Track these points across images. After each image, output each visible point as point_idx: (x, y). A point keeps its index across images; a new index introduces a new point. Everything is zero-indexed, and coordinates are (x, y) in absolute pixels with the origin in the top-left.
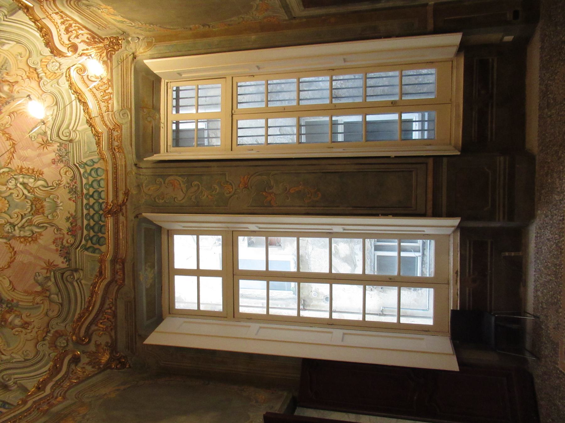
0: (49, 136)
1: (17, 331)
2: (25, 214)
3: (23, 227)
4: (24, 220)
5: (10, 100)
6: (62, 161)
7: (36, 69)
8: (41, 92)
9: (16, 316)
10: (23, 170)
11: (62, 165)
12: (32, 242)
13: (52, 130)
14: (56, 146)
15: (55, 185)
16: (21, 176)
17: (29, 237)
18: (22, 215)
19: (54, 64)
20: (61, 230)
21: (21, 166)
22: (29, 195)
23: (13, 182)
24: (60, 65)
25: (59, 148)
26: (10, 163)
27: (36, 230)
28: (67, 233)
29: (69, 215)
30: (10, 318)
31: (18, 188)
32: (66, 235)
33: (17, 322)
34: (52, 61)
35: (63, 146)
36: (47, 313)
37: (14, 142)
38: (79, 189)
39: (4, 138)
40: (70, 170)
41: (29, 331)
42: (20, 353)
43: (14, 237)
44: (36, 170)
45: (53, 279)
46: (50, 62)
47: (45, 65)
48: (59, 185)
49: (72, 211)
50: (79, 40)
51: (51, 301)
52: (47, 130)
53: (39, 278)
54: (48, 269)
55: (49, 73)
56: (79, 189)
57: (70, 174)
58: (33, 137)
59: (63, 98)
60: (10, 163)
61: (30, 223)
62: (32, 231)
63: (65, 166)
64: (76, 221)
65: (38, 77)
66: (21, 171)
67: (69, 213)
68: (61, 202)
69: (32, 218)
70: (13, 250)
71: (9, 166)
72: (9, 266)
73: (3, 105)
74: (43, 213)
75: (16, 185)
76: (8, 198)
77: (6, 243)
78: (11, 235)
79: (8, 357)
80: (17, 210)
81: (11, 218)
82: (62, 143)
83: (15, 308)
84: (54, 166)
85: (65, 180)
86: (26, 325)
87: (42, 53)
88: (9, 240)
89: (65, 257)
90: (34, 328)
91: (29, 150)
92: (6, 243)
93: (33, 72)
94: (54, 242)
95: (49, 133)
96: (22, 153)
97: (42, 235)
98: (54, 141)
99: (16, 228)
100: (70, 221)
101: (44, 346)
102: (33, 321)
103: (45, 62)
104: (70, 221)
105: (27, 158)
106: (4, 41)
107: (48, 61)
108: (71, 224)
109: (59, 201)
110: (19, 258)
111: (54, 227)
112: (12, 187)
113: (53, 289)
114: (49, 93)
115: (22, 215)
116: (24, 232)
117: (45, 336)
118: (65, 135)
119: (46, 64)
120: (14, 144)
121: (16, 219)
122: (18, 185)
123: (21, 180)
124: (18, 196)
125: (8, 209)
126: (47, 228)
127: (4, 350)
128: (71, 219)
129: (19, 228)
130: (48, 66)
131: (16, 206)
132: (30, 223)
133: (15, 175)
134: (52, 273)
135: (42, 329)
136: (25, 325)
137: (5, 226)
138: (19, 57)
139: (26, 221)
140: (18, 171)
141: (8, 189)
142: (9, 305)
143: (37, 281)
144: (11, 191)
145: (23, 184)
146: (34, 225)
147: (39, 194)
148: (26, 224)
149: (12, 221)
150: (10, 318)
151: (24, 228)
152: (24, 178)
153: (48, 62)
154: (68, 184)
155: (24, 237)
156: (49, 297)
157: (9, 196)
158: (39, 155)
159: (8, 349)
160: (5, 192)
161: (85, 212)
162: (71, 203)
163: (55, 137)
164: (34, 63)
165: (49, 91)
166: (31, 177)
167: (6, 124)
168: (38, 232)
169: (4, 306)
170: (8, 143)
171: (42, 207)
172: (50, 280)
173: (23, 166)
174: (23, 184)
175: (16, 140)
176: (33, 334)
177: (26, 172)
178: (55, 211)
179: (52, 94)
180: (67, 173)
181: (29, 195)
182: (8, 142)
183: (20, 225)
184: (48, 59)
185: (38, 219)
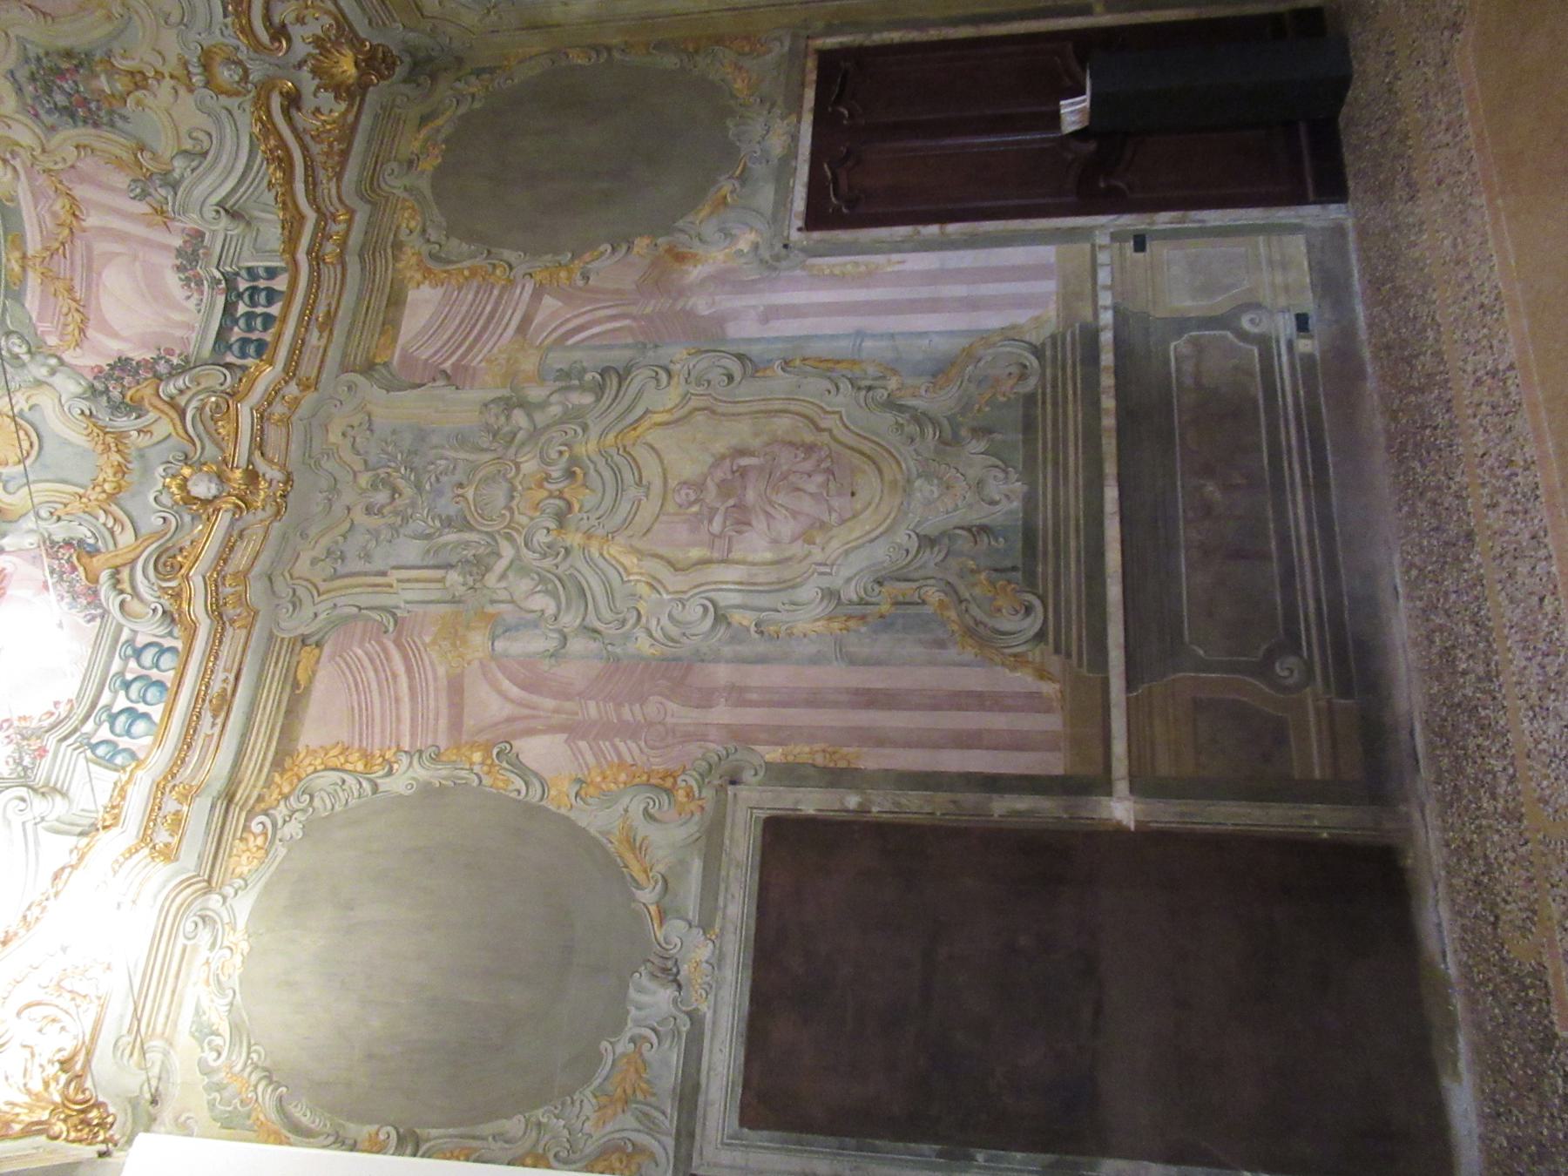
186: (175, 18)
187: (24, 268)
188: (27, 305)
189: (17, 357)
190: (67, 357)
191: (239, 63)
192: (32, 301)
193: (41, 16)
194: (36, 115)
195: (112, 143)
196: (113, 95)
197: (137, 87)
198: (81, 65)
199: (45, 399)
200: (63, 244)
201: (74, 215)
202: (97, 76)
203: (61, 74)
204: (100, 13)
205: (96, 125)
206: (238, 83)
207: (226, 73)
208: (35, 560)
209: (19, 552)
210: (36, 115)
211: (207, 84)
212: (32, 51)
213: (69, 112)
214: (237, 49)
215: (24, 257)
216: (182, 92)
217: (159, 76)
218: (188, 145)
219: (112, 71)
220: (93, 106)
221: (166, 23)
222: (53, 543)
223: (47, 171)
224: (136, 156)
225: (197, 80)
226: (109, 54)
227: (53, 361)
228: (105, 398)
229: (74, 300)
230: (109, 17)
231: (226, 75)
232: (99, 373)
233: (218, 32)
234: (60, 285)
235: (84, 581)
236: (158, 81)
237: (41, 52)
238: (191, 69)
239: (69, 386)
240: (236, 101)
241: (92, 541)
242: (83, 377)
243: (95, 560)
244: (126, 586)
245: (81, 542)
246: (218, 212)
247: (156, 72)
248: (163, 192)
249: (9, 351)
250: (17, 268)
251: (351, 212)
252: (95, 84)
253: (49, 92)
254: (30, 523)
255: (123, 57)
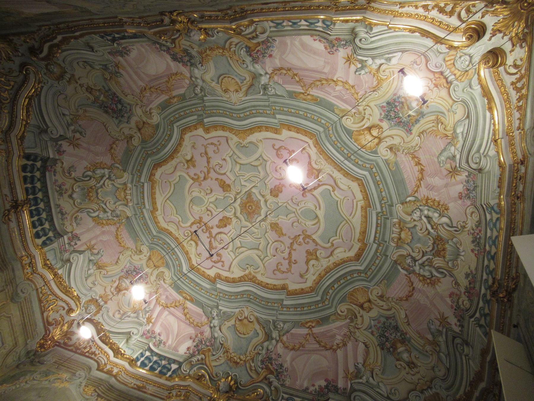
0: (458, 161)
1: (401, 365)
2: (426, 252)
3: (422, 265)
4: (425, 258)
5: (420, 118)
6: (469, 197)
7: (442, 73)
8: (451, 102)
9: (406, 350)
10: (429, 201)
11: (468, 202)
12: (430, 285)
13: (461, 153)
14: (463, 176)
15: (459, 227)
16: (426, 207)
17: (428, 278)
18: (423, 252)
19: (462, 58)
20: (459, 285)
21: (428, 197)
22: (432, 231)
23: (418, 213)
24: (471, 57)
25: (467, 179)
26: (416, 191)
27: (435, 273)
28: (465, 293)
29: (469, 272)
30: (401, 349)
31: (422, 221)
32: (463, 296)
33: (405, 356)
34: (458, 56)
35: (472, 177)
36: (433, 367)
37: (422, 167)
38: (482, 241)
39: (413, 163)
40: (476, 211)
41: (412, 373)
42: (389, 387)
43: (414, 272)
44: (441, 203)
45: (444, 337)
46: (457, 58)
47: (451, 64)
48: (463, 229)
49: (473, 266)
50: (479, 15)
51: (439, 359)
52: (456, 153)
53: (432, 327)
54: (441, 323)
55: (460, 72)
56: (482, 241)
57: (476, 217)
58: (442, 162)
59: (475, 107)
60: (416, 191)
61: (430, 263)
62: (431, 273)
63: (472, 205)
64: (474, 282)
65: (447, 82)
66: (427, 202)
67: (469, 268)
68: (463, 251)
69: (432, 259)
70: (412, 285)
71: (416, 195)
72: (407, 300)
73: (412, 125)
74: (444, 257)
75: (421, 217)
76: (411, 230)
77: (406, 275)
78: (411, 269)
79: (375, 383)
80: (419, 245)
81: (413, 252)
82: (471, 173)
83: (407, 343)
84: (460, 202)
85: (471, 223)
86: (412, 365)
87: (440, 51)
88: (410, 274)
89: (459, 321)
90: (418, 372)
91: (437, 178)
92: (406, 275)
93: (440, 78)
94: (450, 296)
95: (458, 157)
96: (429, 180)
97: (440, 282)
98: (464, 169)
99: (417, 263)
100: (469, 279)
101: (417, 397)
102: (420, 366)
103: (450, 60)
104: (469, 279)
105: (434, 187)
106: (387, 56)
107: (452, 57)
108: (470, 284)
109: (461, 249)
110: (416, 295)
111: (453, 279)
112: (417, 219)
113: (443, 346)
114: (461, 101)
115: (423, 252)
116: (424, 271)
117: (425, 390)
118: (474, 161)
119: (452, 62)
120: (422, 169)
121: (417, 254)
122: (423, 217)
123: (426, 212)
124: (421, 230)
125: (411, 242)
126: (445, 276)
127: (376, 374)
128: (471, 277)
129: (419, 264)
130: (455, 64)
131: (419, 240)
132: (430, 263)
133: (421, 206)
134: (445, 330)
135: (426, 379)
136: (411, 365)
137: (407, 258)
138: (415, 65)
139: (427, 260)
140: (424, 202)
141: (412, 220)
142: (403, 337)
143: (430, 329)
144: (415, 223)
145: (427, 217)
146: (434, 267)
147: (443, 233)
148: (426, 263)
149: (414, 255)
150: (401, 349)
151: (424, 266)
152: (429, 210)
153: (455, 59)
154: (473, 230)
155: (424, 276)
156: (438, 353)
157: (412, 228)
158: (447, 185)
159: (380, 376)
160: (410, 222)
161: (485, 276)
162: (473, 255)
163: (464, 165)
164: (436, 67)
165: (461, 99)
166: (436, 210)
167: (415, 147)
168: (437, 277)
169: (399, 334)
170: (417, 168)
171: (444, 250)
172: (442, 335)
173: (429, 196)
174: (427, 217)
175: (424, 165)
176: (415, 378)
177: (432, 203)
178: (456, 259)
179: (463, 101)
180: (473, 215)
181: (432, 231)
182: (417, 167)
183: (420, 262)
184: (453, 55)
185: (438, 262)
186: (64, 96)
187: (174, 97)
188: (183, 92)
189: (201, 90)
190: (188, 75)
191: (47, 69)
192: (182, 91)
193: (107, 126)
194: (130, 110)
195: (114, 88)
196: (102, 93)
197: (92, 89)
198: (105, 107)
199: (207, 77)
200: (156, 89)
201: (145, 89)
202: (102, 101)
203: (113, 109)
204: (87, 114)
205: (115, 94)
206: (53, 65)
207: (55, 70)
208: (264, 63)
209: (263, 68)
210: (130, 110)
211: (66, 72)
212: (117, 122)
213: (120, 101)
214: (45, 74)
215: (170, 98)
216: (77, 77)
217: (81, 86)
218: (88, 68)
219: (97, 99)
220: (111, 97)
221: (67, 97)
222: (253, 60)
223: (141, 101)
224: (110, 79)
225: (68, 76)
226: (93, 103)
227: (193, 79)
228: (191, 61)
229: (169, 79)
230: (85, 111)
231: (56, 70)
232: (185, 64)
233: (49, 83)
234: (169, 85)
235: (261, 46)
236: (83, 85)
237: (114, 119)
238: (68, 79)
239: (197, 72)
240: (58, 62)
241: (245, 49)
242: (190, 69)
243: (250, 46)
244: (254, 34)
245: (247, 52)
246: (96, 51)
247: (81, 87)
248: (111, 68)
249: (201, 92)
250: (175, 100)
251: (40, 26)
252: (105, 100)
253: (121, 110)
254: (251, 68)
255: (89, 99)
